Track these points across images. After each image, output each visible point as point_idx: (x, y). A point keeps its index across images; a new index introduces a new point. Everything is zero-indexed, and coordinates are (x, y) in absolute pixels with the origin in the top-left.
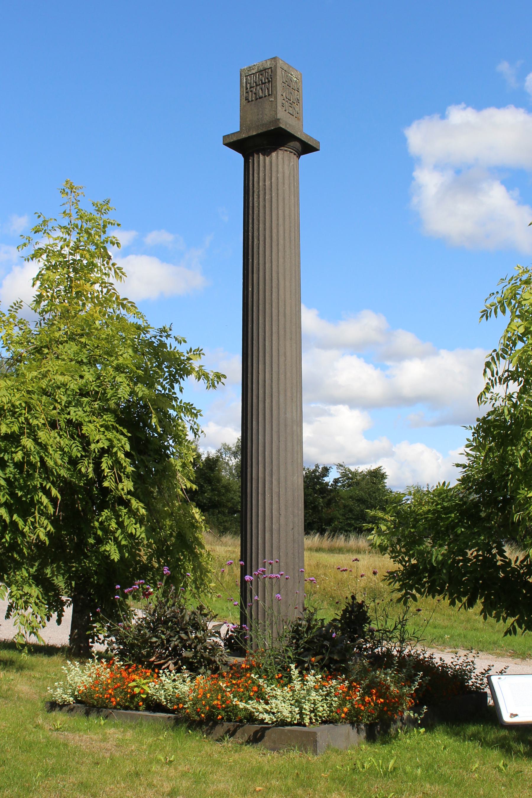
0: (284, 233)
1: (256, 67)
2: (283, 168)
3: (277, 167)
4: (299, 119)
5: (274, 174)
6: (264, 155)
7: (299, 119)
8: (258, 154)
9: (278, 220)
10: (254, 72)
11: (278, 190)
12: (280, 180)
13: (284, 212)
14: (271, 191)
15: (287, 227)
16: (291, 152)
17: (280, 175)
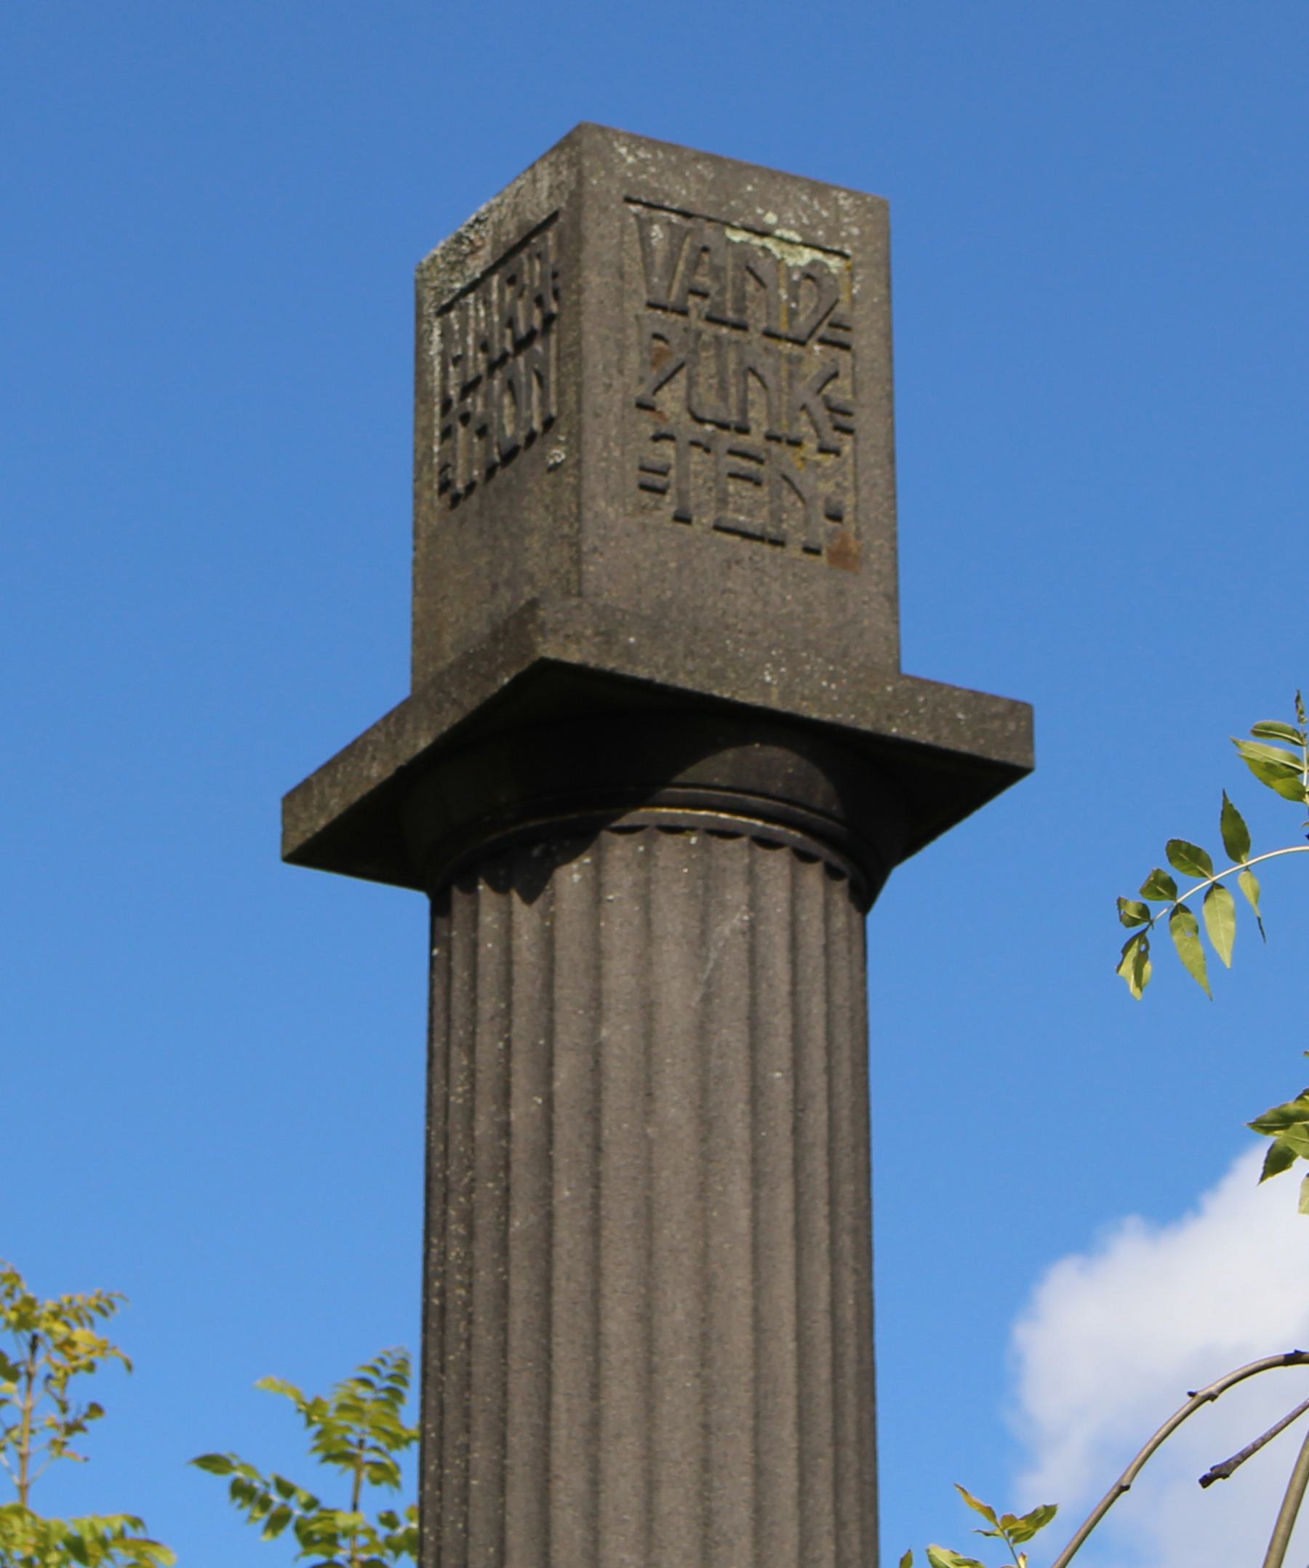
0: (651, 1486)
1: (487, 232)
2: (645, 965)
3: (597, 971)
4: (843, 558)
5: (569, 1031)
6: (501, 887)
7: (843, 558)
8: (471, 889)
9: (596, 1389)
10: (476, 267)
11: (597, 1149)
12: (618, 1072)
13: (647, 1316)
14: (547, 1164)
15: (678, 1441)
16: (768, 843)
17: (618, 1034)
